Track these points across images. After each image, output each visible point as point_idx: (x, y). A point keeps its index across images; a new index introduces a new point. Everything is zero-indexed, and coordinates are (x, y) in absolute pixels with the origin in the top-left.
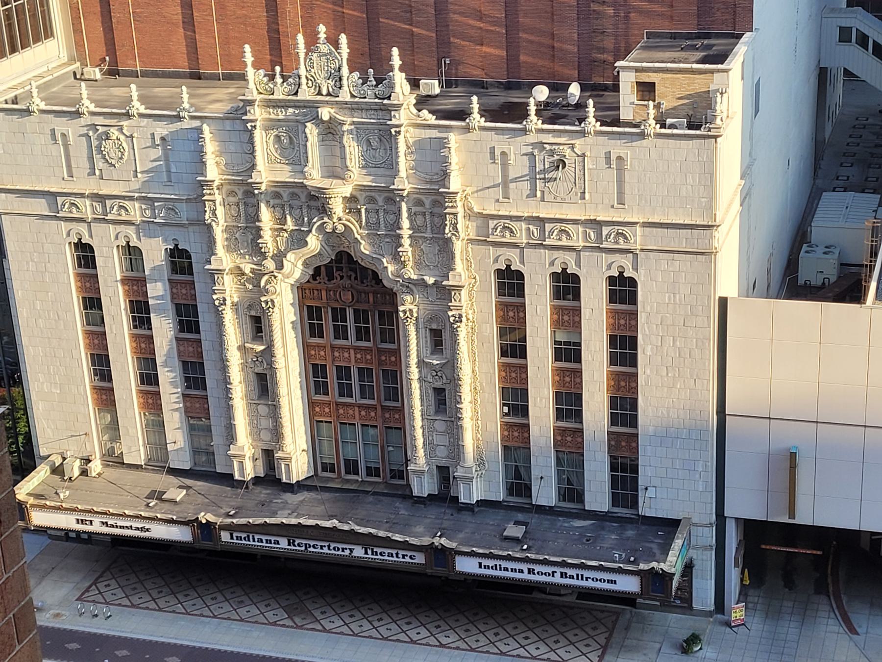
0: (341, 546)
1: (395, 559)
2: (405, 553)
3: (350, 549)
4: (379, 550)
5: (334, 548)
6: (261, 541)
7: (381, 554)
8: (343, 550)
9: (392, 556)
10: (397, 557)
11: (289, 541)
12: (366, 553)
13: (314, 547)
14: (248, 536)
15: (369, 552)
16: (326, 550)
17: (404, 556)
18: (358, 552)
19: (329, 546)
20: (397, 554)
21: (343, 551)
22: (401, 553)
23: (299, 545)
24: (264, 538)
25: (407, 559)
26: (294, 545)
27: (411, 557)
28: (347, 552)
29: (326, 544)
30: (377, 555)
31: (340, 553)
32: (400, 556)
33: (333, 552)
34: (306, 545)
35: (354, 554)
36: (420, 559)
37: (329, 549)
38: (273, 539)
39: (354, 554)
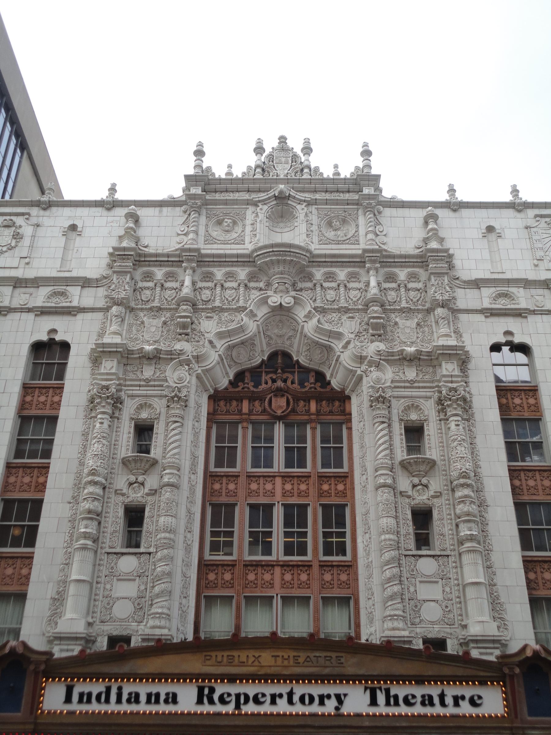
0: (316, 690)
1: (438, 710)
2: (458, 691)
3: (338, 697)
4: (400, 691)
5: (302, 699)
6: (135, 698)
7: (407, 702)
8: (322, 700)
9: (432, 704)
10: (443, 704)
11: (201, 690)
13: (257, 701)
14: (108, 690)
15: (381, 698)
16: (282, 706)
17: (457, 700)
18: (357, 701)
19: (290, 695)
20: (442, 697)
21: (322, 703)
22: (451, 691)
24: (143, 689)
25: (466, 709)
26: (211, 702)
27: (473, 702)
28: (330, 706)
29: (284, 689)
30: (397, 704)
31: (315, 708)
32: (449, 700)
33: (299, 709)
34: (238, 696)
35: (346, 710)
36: (493, 702)
37: (290, 702)
38: (163, 689)
39: (348, 708)
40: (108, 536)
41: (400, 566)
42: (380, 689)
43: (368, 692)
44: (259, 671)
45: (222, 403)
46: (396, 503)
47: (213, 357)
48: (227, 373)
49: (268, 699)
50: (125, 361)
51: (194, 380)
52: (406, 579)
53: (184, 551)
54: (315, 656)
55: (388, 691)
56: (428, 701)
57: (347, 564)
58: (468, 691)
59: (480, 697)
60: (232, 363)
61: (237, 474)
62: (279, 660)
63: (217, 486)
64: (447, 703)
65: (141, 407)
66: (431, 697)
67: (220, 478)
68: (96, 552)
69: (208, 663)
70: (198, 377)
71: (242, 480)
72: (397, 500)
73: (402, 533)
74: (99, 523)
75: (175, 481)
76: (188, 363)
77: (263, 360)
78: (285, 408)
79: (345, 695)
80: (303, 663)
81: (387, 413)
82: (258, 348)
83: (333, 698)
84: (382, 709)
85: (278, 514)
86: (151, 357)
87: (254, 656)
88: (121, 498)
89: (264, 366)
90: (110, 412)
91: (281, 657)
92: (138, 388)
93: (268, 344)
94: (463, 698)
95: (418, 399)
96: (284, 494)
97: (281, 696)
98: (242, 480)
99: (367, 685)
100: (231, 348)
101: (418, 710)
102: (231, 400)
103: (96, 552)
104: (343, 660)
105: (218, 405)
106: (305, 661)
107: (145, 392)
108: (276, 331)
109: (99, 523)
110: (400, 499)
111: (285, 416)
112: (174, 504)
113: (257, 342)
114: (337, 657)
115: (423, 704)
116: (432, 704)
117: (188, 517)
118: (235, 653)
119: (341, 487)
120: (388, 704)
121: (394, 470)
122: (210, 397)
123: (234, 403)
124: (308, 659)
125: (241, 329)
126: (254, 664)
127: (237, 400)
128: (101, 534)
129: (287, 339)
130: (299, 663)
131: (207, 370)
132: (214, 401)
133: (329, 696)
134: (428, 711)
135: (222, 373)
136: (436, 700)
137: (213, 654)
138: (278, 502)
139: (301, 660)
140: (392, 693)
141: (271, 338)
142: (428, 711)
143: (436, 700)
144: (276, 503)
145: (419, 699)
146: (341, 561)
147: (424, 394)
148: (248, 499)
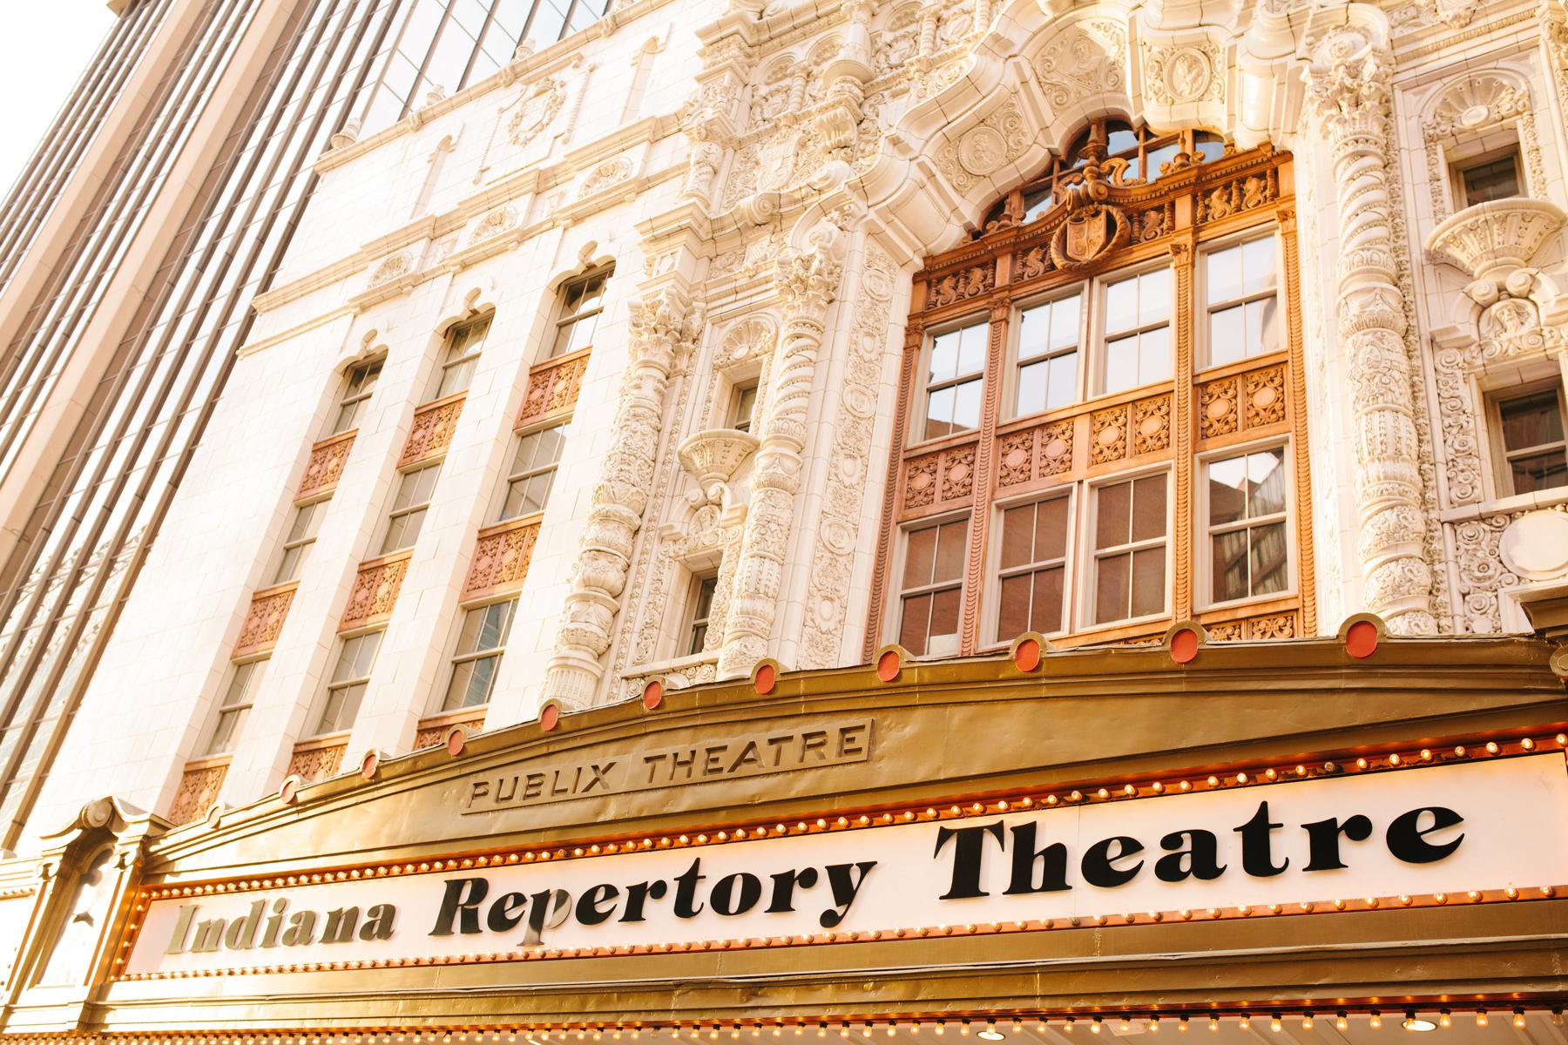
0: (766, 859)
1: (1236, 892)
4: (1072, 829)
5: (720, 900)
7: (1099, 870)
9: (1207, 867)
12: (966, 884)
13: (588, 913)
15: (997, 863)
16: (661, 926)
17: (1325, 846)
20: (1257, 835)
21: (782, 903)
22: (1298, 805)
23: (500, 922)
25: (1372, 875)
26: (470, 926)
27: (1407, 842)
30: (1056, 881)
32: (1290, 846)
33: (709, 928)
35: (862, 920)
37: (684, 909)
40: (635, 638)
41: (1430, 557)
42: (998, 830)
43: (951, 847)
44: (598, 814)
45: (947, 284)
46: (1414, 372)
47: (903, 173)
48: (955, 210)
49: (622, 902)
50: (709, 249)
51: (858, 241)
52: (1457, 599)
53: (805, 645)
54: (772, 742)
55: (1026, 835)
56: (1194, 856)
57: (1282, 607)
58: (1382, 797)
59: (1446, 818)
60: (962, 180)
61: (972, 438)
62: (664, 768)
63: (922, 481)
64: (1277, 862)
65: (738, 336)
66: (1205, 843)
67: (930, 459)
68: (599, 681)
69: (480, 804)
70: (873, 233)
71: (988, 449)
72: (1416, 362)
73: (1440, 457)
74: (616, 614)
75: (780, 471)
76: (837, 203)
77: (1053, 155)
78: (1101, 241)
79: (866, 868)
80: (732, 769)
81: (1376, 130)
82: (1030, 125)
83: (824, 882)
84: (998, 907)
85: (1082, 515)
86: (760, 220)
87: (595, 768)
88: (672, 548)
89: (1056, 166)
90: (666, 362)
91: (670, 758)
92: (732, 298)
93: (1058, 106)
94: (1359, 828)
95: (1493, 65)
96: (1098, 457)
97: (659, 889)
98: (988, 449)
99: (949, 825)
100: (951, 142)
101: (1149, 897)
102: (968, 270)
103: (599, 681)
104: (861, 739)
105: (938, 293)
106: (742, 760)
107: (747, 301)
108: (1073, 69)
109: (616, 614)
110: (1428, 360)
111: (1104, 259)
112: (773, 526)
113: (1023, 106)
114: (844, 731)
115: (1168, 871)
116: (1207, 867)
117: (826, 561)
118: (545, 768)
119: (1265, 397)
120: (1020, 884)
121: (1405, 281)
122: (917, 278)
123: (977, 274)
124: (750, 755)
125: (971, 84)
126: (592, 792)
127: (983, 266)
128: (618, 637)
129: (1107, 77)
130: (721, 770)
131: (892, 210)
132: (929, 285)
133: (809, 878)
134: (1191, 898)
135: (940, 210)
136: (1230, 852)
137: (492, 778)
138: (1080, 482)
139: (726, 760)
140: (1043, 842)
141: (1065, 91)
142: (1191, 898)
143: (1230, 852)
144: (1075, 485)
145: (1154, 854)
146: (1266, 603)
147: (1512, 40)
148: (998, 494)
